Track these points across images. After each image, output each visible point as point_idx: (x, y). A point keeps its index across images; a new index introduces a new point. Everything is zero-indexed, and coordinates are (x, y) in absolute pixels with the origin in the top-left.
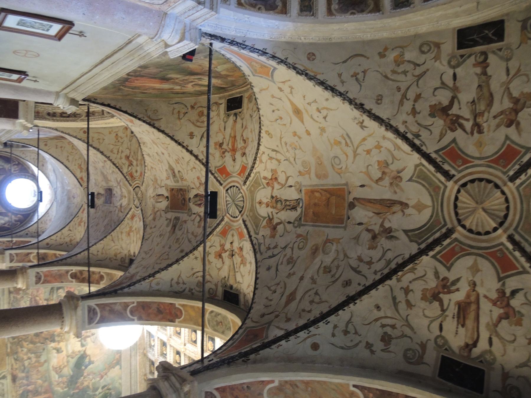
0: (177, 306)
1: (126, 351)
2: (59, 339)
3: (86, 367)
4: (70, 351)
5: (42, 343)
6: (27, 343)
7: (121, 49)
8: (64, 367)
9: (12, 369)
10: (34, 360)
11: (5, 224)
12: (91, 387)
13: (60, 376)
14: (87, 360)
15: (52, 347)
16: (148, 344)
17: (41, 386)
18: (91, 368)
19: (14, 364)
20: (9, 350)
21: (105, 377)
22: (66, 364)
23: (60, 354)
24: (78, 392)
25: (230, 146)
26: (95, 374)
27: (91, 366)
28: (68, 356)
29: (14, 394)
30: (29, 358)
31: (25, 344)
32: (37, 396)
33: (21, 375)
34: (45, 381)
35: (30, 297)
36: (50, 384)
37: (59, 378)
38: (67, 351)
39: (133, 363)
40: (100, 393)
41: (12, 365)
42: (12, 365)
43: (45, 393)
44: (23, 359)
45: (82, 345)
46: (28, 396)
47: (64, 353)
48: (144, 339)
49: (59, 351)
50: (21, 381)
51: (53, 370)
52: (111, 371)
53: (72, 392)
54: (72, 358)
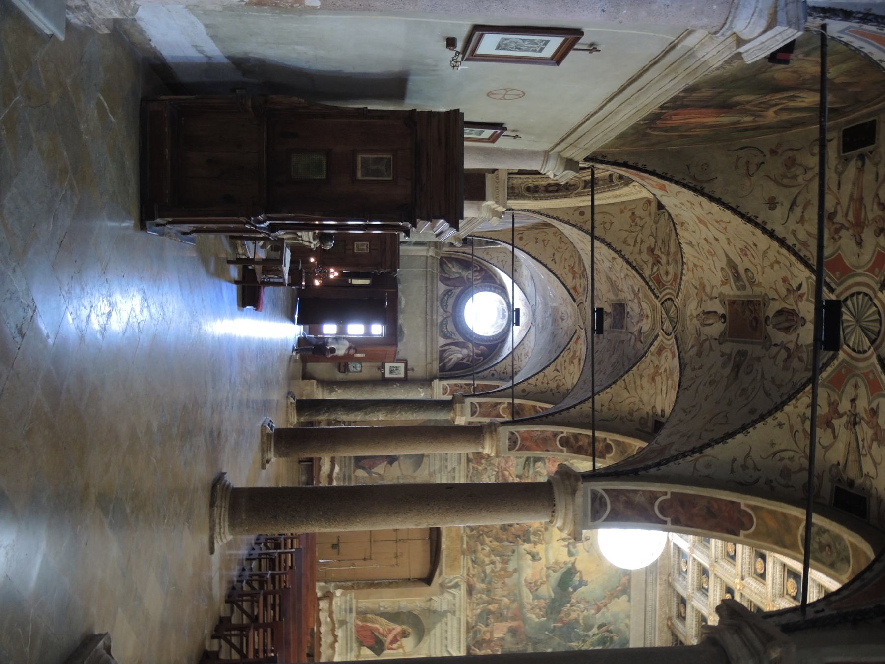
0: (743, 507)
1: (638, 572)
3: (575, 590)
4: (552, 561)
5: (511, 542)
7: (655, 63)
9: (468, 575)
10: (499, 566)
11: (462, 359)
12: (581, 621)
13: (537, 597)
14: (577, 578)
16: (676, 567)
17: (508, 608)
19: (471, 568)
20: (465, 546)
21: (604, 610)
22: (545, 579)
24: (560, 628)
25: (851, 217)
26: (588, 602)
27: (583, 589)
28: (548, 568)
29: (469, 613)
30: (493, 563)
31: (487, 540)
32: (501, 621)
33: (480, 586)
34: (513, 601)
36: (521, 606)
38: (547, 558)
39: (649, 596)
40: (594, 635)
41: (468, 569)
42: (468, 569)
43: (514, 618)
44: (483, 562)
45: (570, 554)
46: (488, 619)
47: (543, 561)
48: (669, 558)
49: (535, 557)
50: (479, 595)
51: (526, 586)
52: (613, 602)
53: (552, 625)
54: (555, 571)
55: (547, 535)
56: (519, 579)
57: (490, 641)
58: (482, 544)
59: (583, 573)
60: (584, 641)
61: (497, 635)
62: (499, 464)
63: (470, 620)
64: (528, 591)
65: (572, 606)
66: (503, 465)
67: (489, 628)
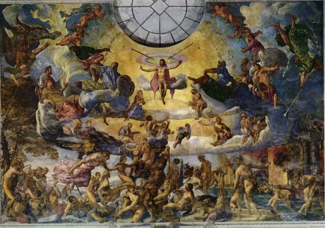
2: (161, 131)
3: (230, 78)
5: (165, 164)
6: (159, 191)
8: (220, 123)
9: (204, 220)
10: (195, 179)
12: (272, 69)
15: (175, 146)
18: (234, 67)
19: (196, 215)
21: (258, 38)
22: (214, 119)
23: (193, 131)
27: (229, 68)
28: (200, 115)
29: (254, 217)
30: (190, 188)
32: (267, 176)
34: (241, 159)
35: (71, 185)
36: (249, 150)
37: (240, 134)
38: (188, 116)
40: (292, 50)
42: (197, 219)
44: (188, 199)
45: (183, 86)
47: (191, 121)
50: (232, 205)
52: (248, 26)
54: (205, 106)
55: (158, 117)
56: (212, 153)
57: (293, 190)
58: (166, 202)
59: (208, 68)
60: (300, 64)
61: (284, 179)
62: (64, 182)
63: (264, 216)
64: (229, 141)
65: (251, 82)
66: (65, 176)
67: (276, 191)
